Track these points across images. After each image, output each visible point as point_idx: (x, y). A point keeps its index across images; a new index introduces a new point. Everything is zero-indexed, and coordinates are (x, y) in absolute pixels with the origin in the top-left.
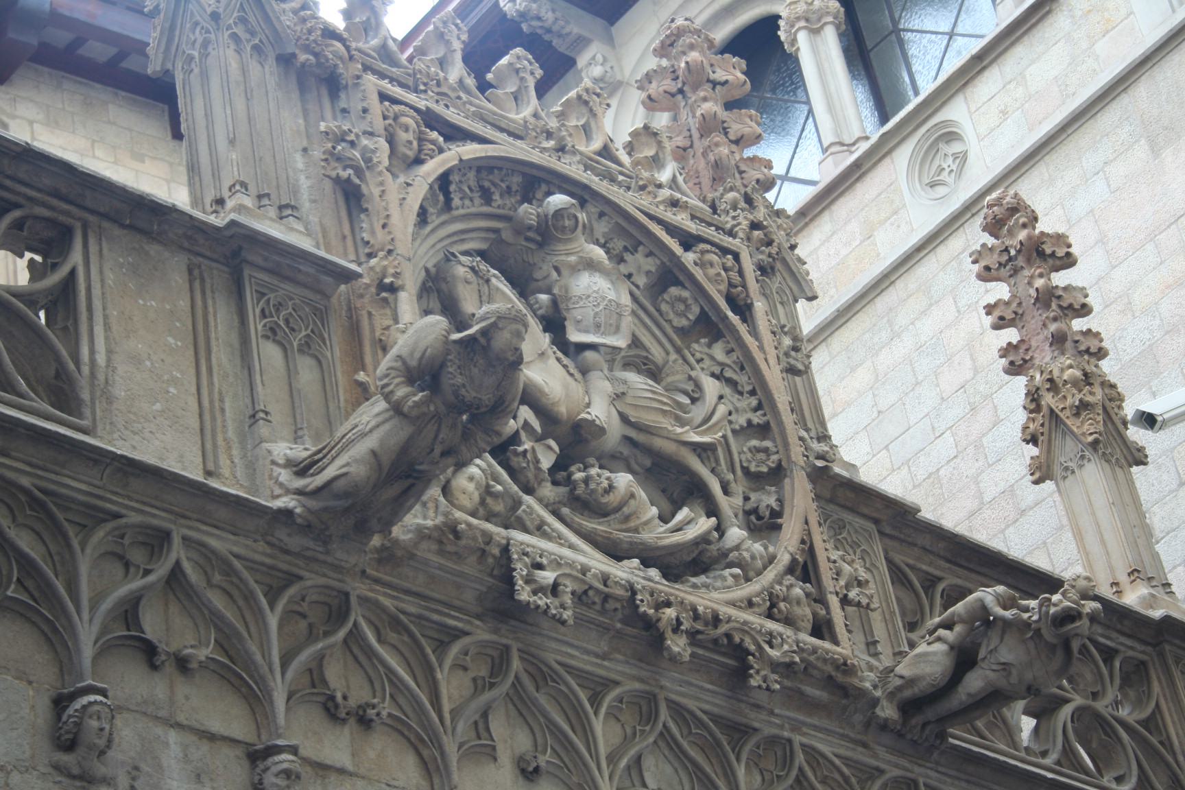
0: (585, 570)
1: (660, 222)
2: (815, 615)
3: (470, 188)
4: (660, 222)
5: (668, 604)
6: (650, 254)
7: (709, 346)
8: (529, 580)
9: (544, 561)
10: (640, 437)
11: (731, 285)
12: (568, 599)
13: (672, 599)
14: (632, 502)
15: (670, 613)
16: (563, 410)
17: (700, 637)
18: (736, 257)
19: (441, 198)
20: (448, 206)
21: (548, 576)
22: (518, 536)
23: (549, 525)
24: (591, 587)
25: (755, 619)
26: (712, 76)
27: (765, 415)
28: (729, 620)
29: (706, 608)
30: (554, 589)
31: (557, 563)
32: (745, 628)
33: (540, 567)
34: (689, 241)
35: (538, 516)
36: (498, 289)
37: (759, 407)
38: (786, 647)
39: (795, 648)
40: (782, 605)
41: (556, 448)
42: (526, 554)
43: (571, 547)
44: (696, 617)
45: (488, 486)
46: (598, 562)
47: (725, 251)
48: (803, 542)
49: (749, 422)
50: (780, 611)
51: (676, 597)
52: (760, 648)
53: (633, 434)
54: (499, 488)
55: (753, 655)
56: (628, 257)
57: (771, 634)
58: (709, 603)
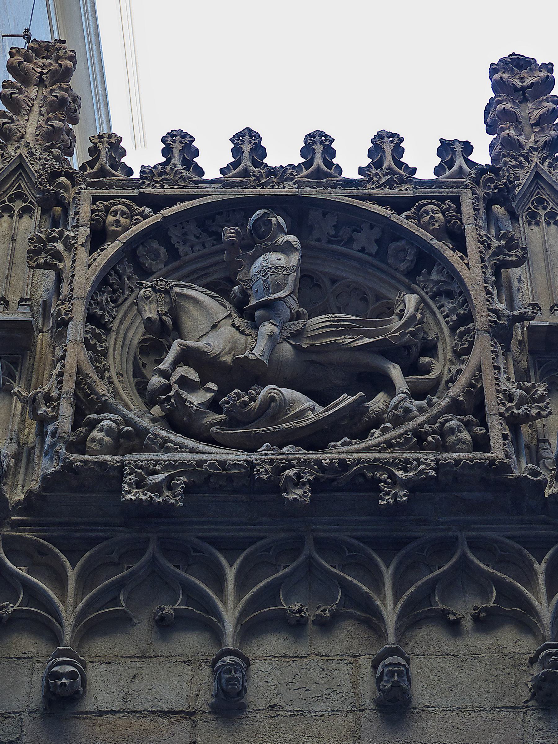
0: (200, 463)
1: (371, 199)
2: (474, 437)
3: (195, 236)
4: (371, 199)
5: (291, 466)
6: (372, 227)
7: (429, 273)
8: (140, 484)
9: (158, 467)
10: (320, 358)
11: (448, 221)
12: (179, 490)
13: (294, 462)
14: (273, 404)
15: (291, 472)
16: (227, 359)
17: (335, 483)
18: (456, 200)
19: (163, 251)
20: (173, 254)
21: (159, 477)
22: (129, 457)
23: (171, 442)
24: (210, 475)
25: (388, 455)
26: (519, 84)
27: (468, 305)
28: (359, 461)
29: (331, 460)
30: (169, 484)
31: (168, 466)
32: (375, 465)
33: (155, 472)
34: (400, 204)
35: (162, 438)
36: (180, 295)
37: (465, 301)
38: (422, 467)
39: (433, 465)
40: (430, 438)
41: (215, 388)
42: (141, 468)
43: (192, 451)
44: (323, 469)
45: (120, 430)
46: (215, 454)
47: (442, 199)
48: (471, 385)
49: (458, 315)
50: (430, 443)
51: (299, 459)
52: (392, 475)
53: (314, 357)
54: (127, 428)
55: (385, 482)
56: (356, 235)
57: (406, 461)
58: (336, 456)
